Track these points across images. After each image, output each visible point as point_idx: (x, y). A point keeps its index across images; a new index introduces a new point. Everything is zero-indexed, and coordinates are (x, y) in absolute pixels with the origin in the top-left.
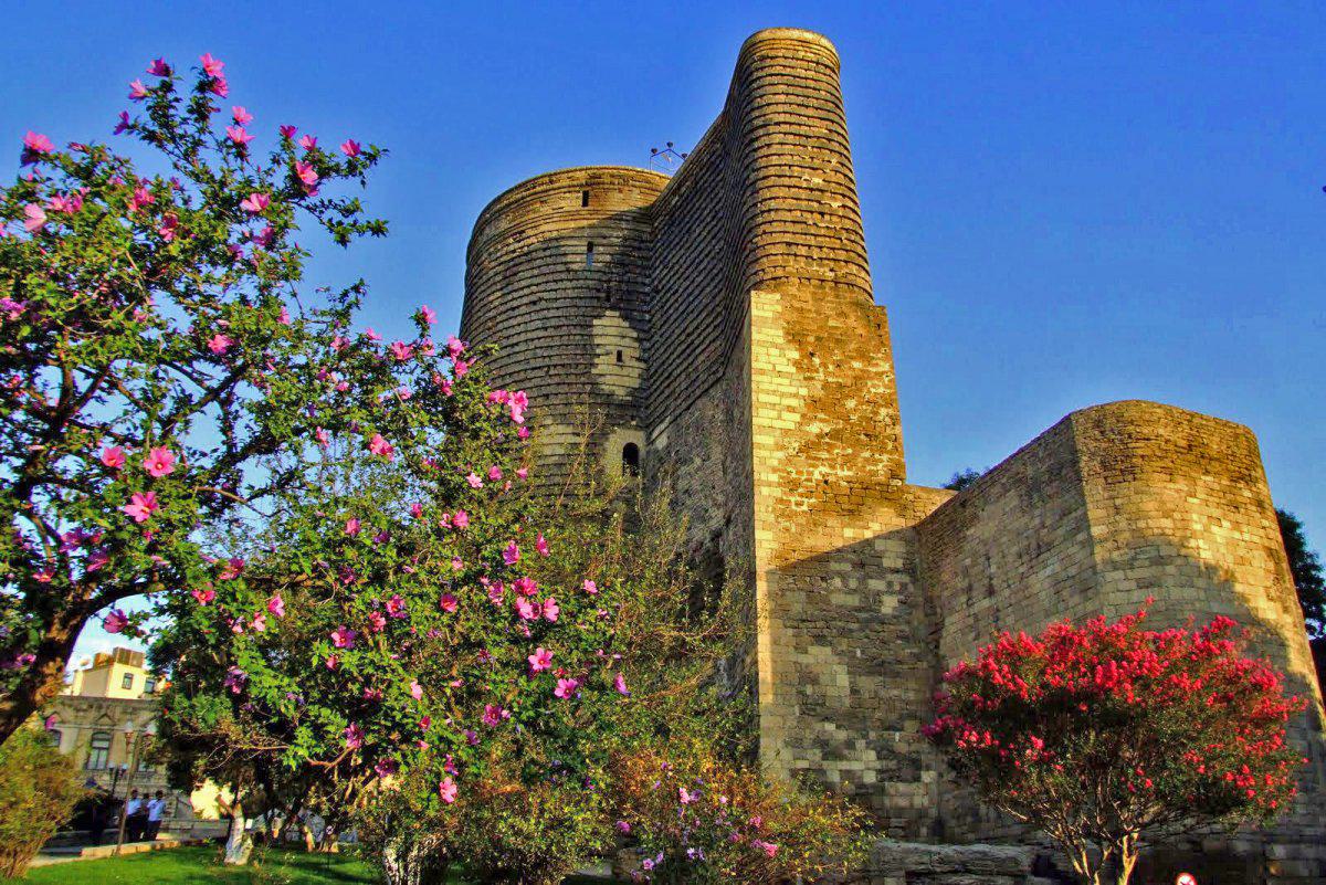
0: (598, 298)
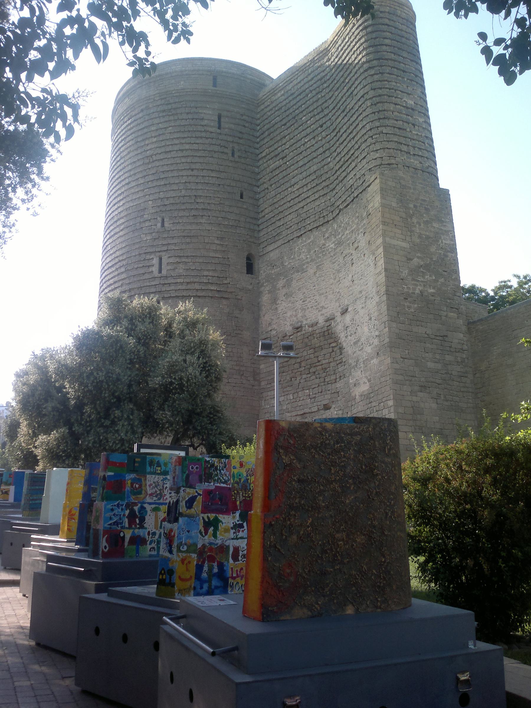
0: (227, 153)
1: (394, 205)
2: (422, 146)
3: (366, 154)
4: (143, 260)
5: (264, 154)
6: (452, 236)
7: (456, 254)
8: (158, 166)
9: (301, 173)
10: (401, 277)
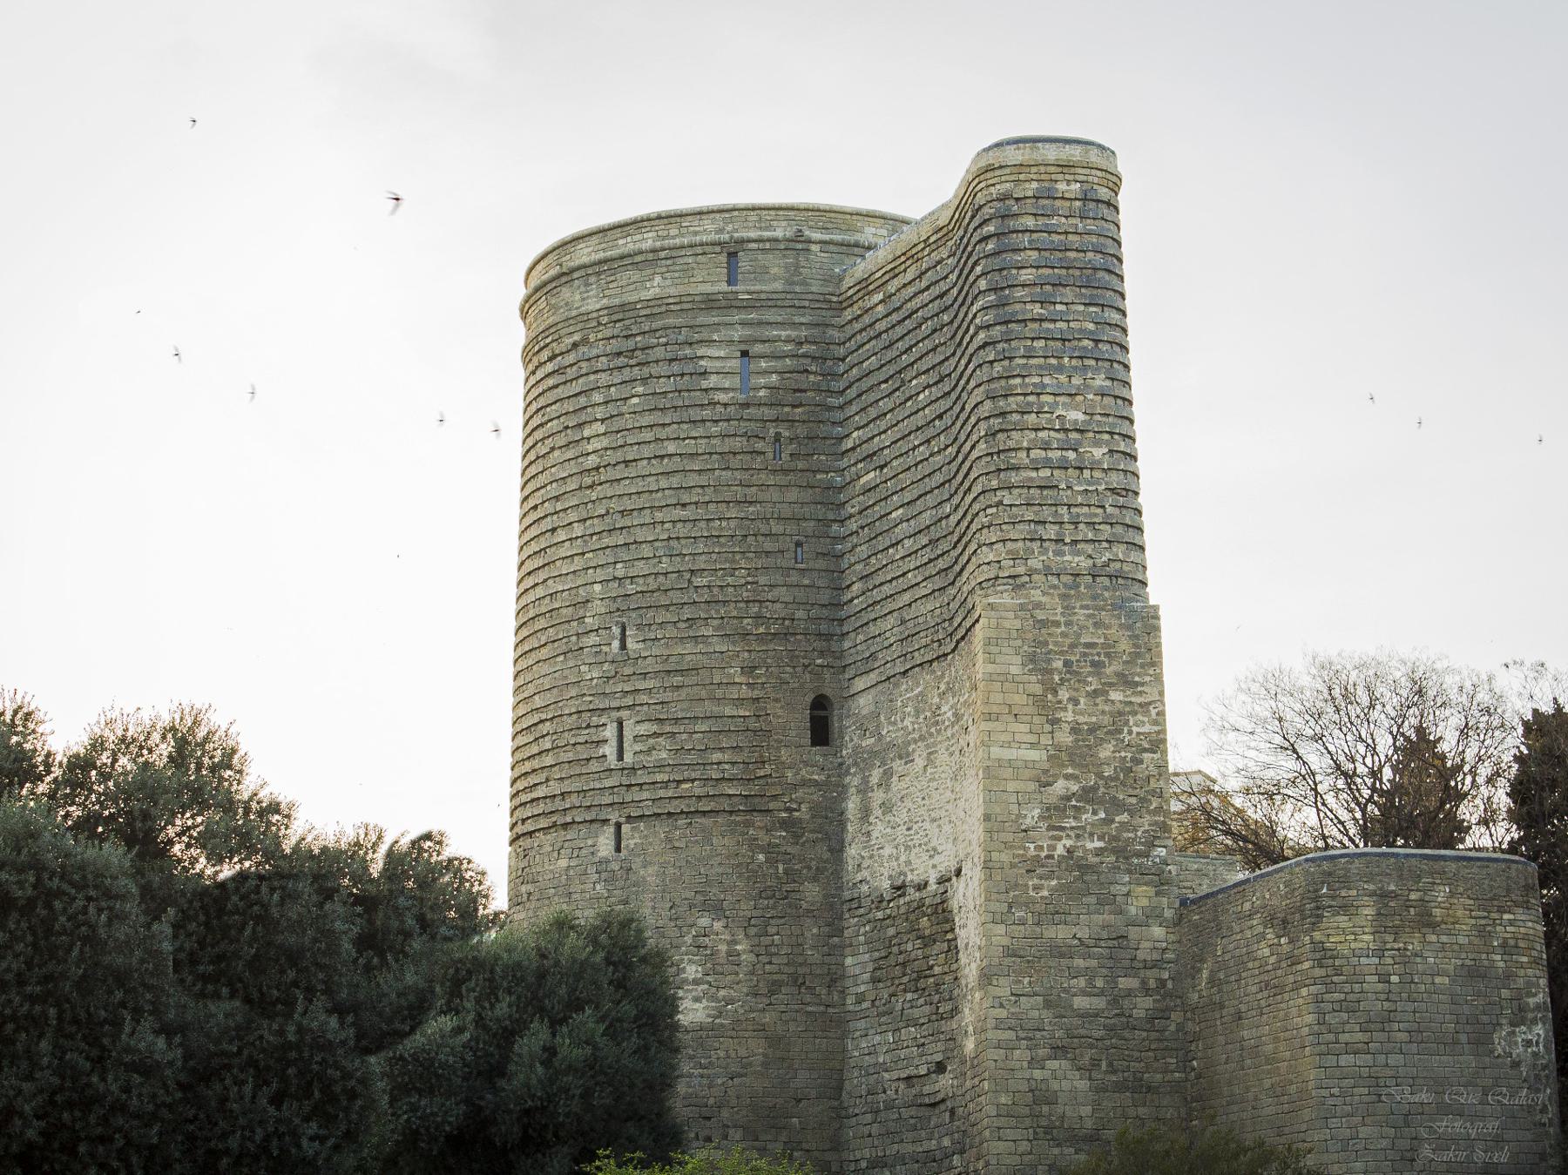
1: (1014, 670)
2: (1096, 515)
3: (976, 546)
4: (586, 728)
5: (849, 444)
6: (1158, 714)
7: (1165, 752)
8: (611, 497)
9: (908, 520)
10: (1023, 827)
